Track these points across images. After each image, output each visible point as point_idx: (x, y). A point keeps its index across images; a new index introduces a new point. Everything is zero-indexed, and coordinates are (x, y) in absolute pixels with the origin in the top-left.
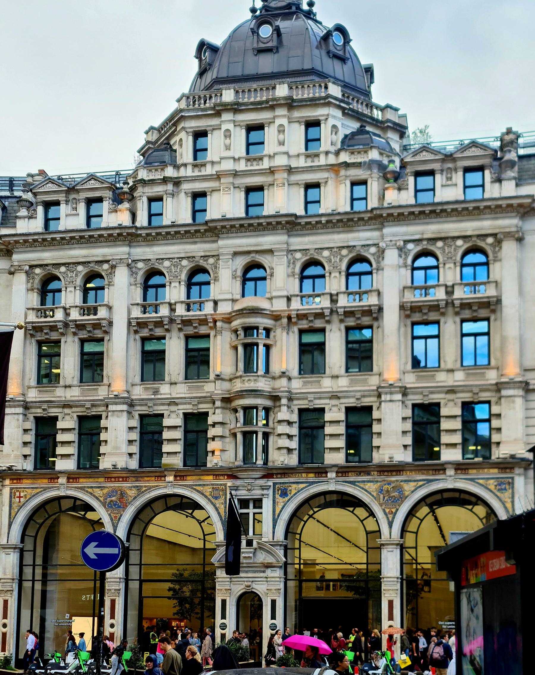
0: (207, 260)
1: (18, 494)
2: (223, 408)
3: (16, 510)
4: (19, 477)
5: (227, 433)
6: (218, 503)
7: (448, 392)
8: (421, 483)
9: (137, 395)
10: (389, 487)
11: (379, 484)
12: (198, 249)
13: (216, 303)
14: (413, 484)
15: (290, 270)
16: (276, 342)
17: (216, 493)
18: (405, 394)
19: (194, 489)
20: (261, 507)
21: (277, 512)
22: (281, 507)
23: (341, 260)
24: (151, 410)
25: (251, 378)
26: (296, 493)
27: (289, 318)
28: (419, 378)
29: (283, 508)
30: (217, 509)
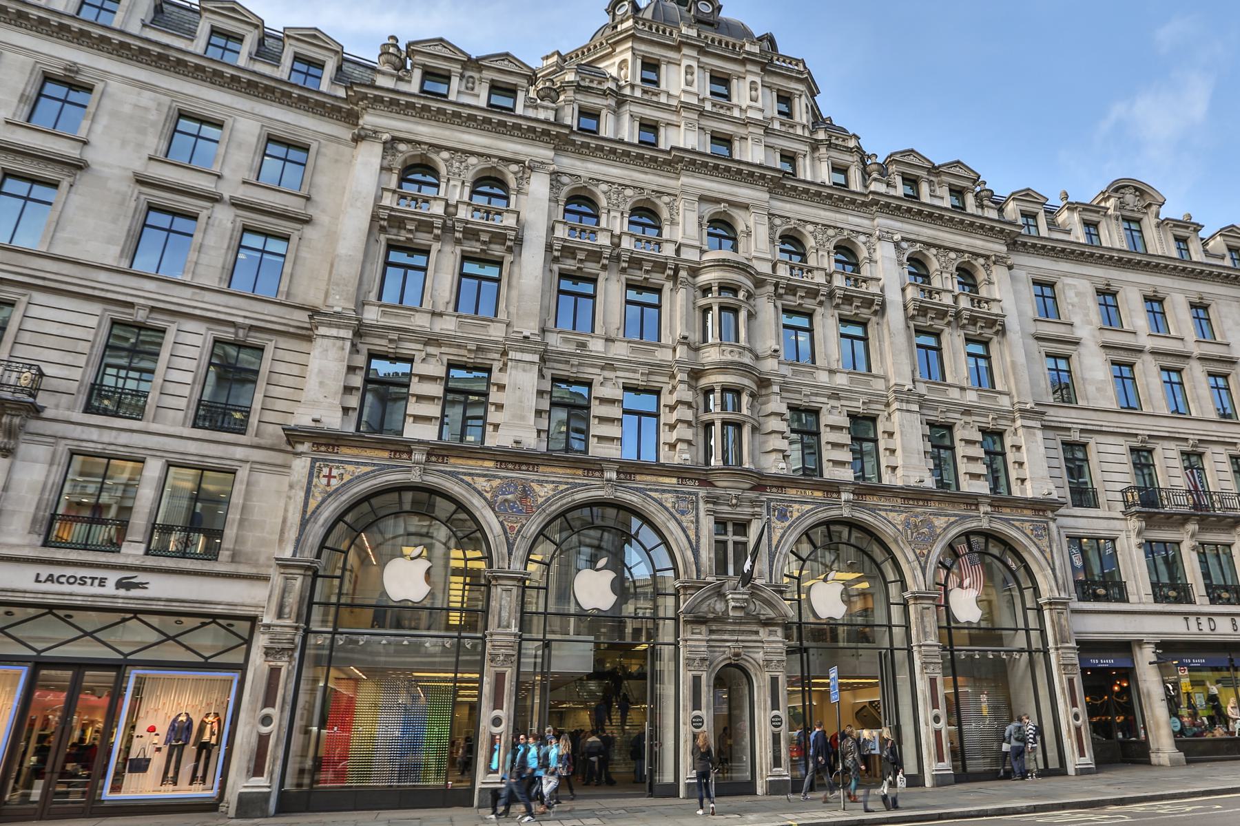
1: (326, 471)
3: (320, 499)
4: (333, 442)
6: (687, 520)
8: (952, 519)
17: (683, 505)
24: (575, 370)
27: (776, 285)
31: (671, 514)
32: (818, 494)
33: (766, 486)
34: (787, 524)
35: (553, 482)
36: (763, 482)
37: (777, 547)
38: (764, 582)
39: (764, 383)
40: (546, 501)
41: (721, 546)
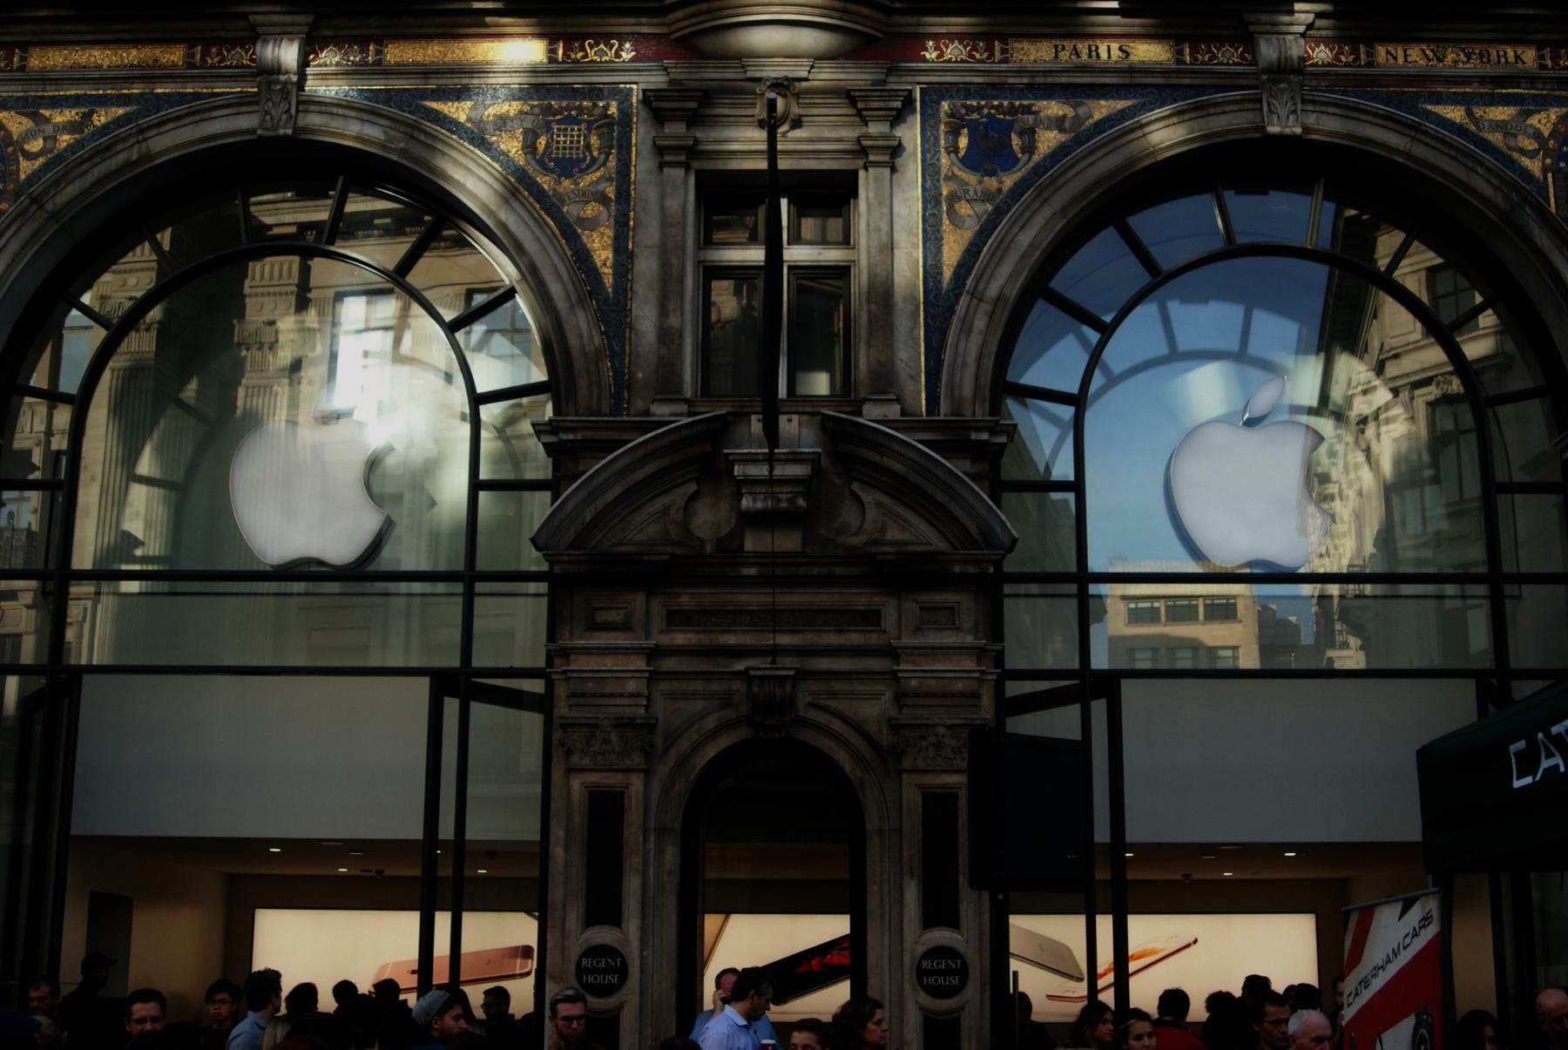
34: (1009, 181)
35: (75, 101)
38: (893, 411)
40: (46, 167)
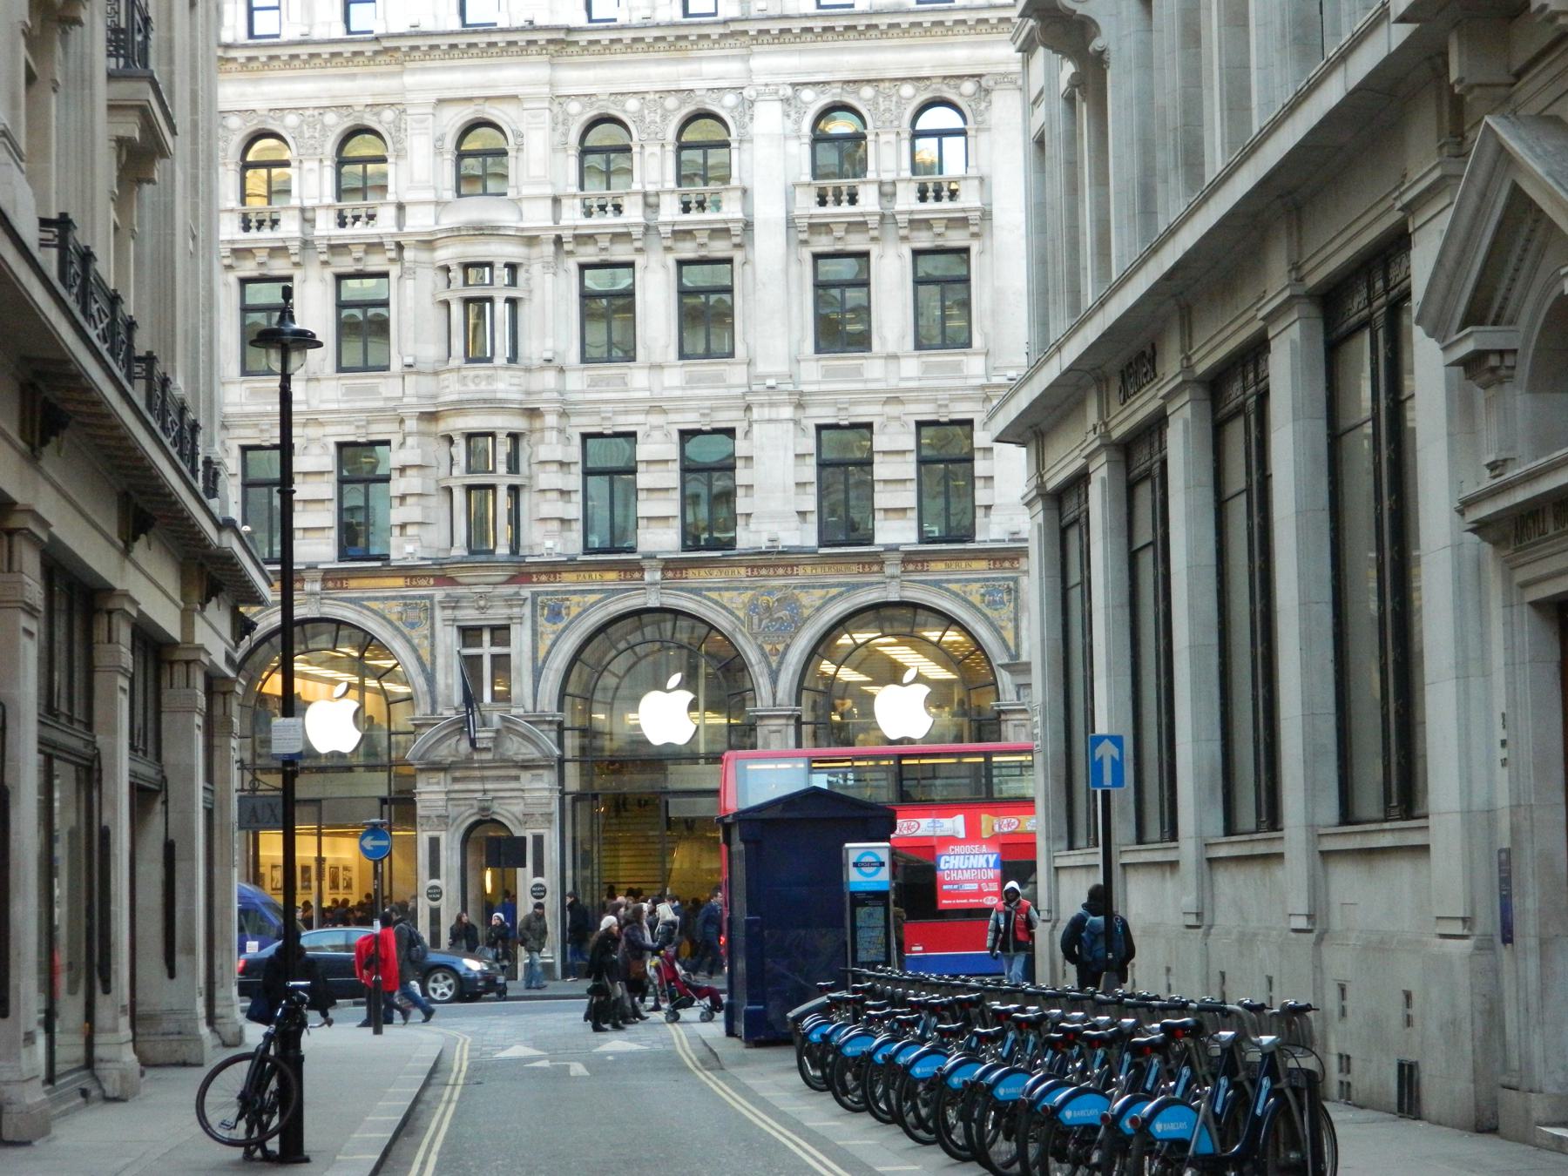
0: (378, 114)
2: (421, 434)
5: (431, 487)
6: (417, 636)
7: (888, 401)
8: (834, 591)
9: (235, 405)
10: (772, 599)
11: (750, 593)
12: (359, 89)
13: (401, 207)
14: (818, 593)
15: (557, 138)
16: (530, 291)
17: (413, 615)
18: (800, 406)
19: (368, 609)
20: (507, 643)
21: (541, 654)
22: (548, 642)
23: (664, 117)
25: (482, 372)
26: (580, 614)
28: (829, 374)
29: (553, 644)
30: (414, 649)
31: (397, 629)
32: (612, 575)
33: (530, 574)
34: (561, 625)
36: (526, 570)
37: (544, 662)
38: (521, 711)
39: (533, 413)
41: (471, 665)
